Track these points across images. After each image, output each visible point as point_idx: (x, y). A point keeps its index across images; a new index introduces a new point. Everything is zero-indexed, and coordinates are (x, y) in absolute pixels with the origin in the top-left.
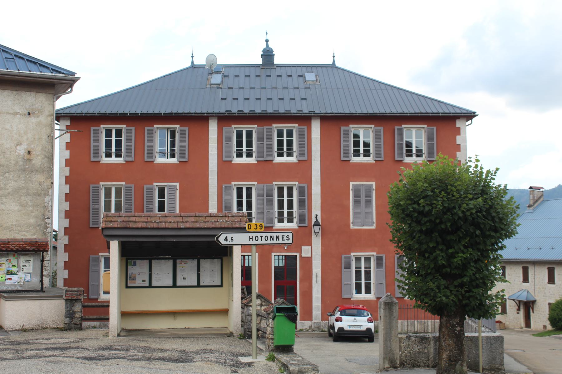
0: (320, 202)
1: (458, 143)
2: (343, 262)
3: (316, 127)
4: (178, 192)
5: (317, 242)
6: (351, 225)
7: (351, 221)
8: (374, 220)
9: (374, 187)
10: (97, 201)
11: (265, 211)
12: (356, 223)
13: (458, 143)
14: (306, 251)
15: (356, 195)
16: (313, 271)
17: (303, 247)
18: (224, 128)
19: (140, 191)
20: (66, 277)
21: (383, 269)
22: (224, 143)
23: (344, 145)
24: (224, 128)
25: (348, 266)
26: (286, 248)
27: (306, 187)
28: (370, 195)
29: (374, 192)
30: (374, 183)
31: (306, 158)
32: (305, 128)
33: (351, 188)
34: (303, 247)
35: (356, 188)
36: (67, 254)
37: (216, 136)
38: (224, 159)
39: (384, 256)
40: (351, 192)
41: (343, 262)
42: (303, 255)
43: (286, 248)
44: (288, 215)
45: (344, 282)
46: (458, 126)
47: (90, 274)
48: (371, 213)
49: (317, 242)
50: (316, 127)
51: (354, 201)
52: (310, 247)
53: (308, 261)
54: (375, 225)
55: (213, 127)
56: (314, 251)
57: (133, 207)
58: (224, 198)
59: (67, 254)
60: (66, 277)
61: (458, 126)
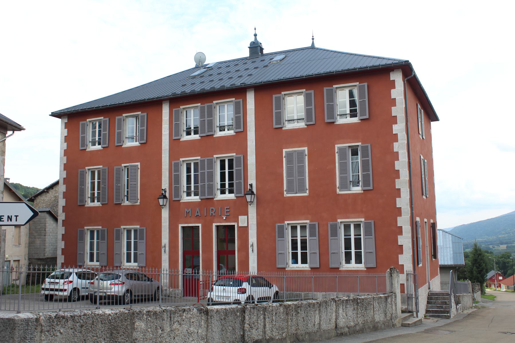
0: (255, 172)
1: (393, 97)
2: (277, 230)
3: (251, 98)
4: (139, 170)
5: (252, 211)
6: (285, 193)
7: (285, 188)
8: (307, 187)
9: (306, 153)
10: (83, 183)
11: (206, 183)
12: (289, 191)
13: (393, 97)
14: (242, 221)
15: (289, 162)
16: (250, 241)
17: (240, 217)
18: (174, 110)
19: (111, 171)
20: (63, 247)
21: (317, 238)
22: (174, 123)
23: (276, 112)
24: (174, 110)
25: (282, 234)
26: (224, 218)
27: (242, 158)
28: (303, 161)
29: (307, 157)
30: (306, 149)
31: (242, 130)
32: (241, 100)
33: (284, 155)
34: (240, 217)
35: (289, 155)
36: (64, 228)
37: (168, 118)
38: (174, 138)
39: (317, 223)
40: (284, 159)
41: (277, 230)
42: (240, 225)
43: (224, 218)
44: (229, 187)
45: (278, 251)
46: (392, 79)
47: (78, 244)
48: (304, 180)
49: (252, 211)
50: (251, 98)
51: (288, 168)
52: (246, 217)
53: (245, 230)
54: (308, 191)
55: (166, 110)
56: (250, 221)
57: (107, 186)
58: (173, 174)
59: (64, 228)
60: (63, 247)
61: (392, 79)
